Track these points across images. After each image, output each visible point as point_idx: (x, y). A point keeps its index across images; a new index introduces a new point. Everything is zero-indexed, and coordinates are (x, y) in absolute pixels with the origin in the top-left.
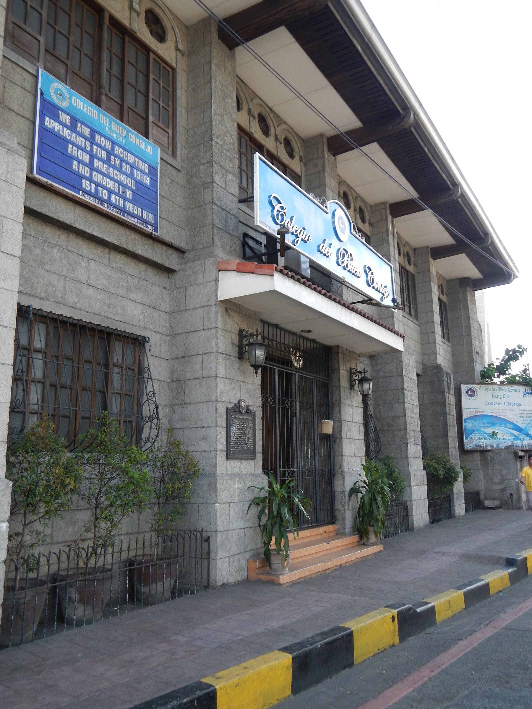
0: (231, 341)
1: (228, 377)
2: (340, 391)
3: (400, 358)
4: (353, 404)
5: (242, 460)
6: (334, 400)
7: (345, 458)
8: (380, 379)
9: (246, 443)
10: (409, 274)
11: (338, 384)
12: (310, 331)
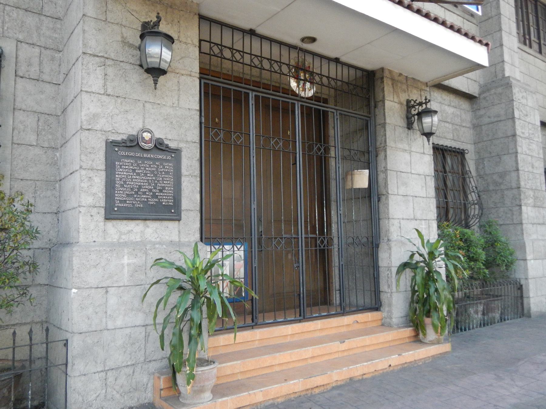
0: (119, 39)
1: (109, 91)
2: (385, 130)
3: (510, 95)
4: (412, 149)
5: (148, 222)
6: (378, 144)
7: (396, 222)
8: (483, 127)
9: (154, 196)
10: (538, 3)
11: (383, 122)
12: (313, 40)
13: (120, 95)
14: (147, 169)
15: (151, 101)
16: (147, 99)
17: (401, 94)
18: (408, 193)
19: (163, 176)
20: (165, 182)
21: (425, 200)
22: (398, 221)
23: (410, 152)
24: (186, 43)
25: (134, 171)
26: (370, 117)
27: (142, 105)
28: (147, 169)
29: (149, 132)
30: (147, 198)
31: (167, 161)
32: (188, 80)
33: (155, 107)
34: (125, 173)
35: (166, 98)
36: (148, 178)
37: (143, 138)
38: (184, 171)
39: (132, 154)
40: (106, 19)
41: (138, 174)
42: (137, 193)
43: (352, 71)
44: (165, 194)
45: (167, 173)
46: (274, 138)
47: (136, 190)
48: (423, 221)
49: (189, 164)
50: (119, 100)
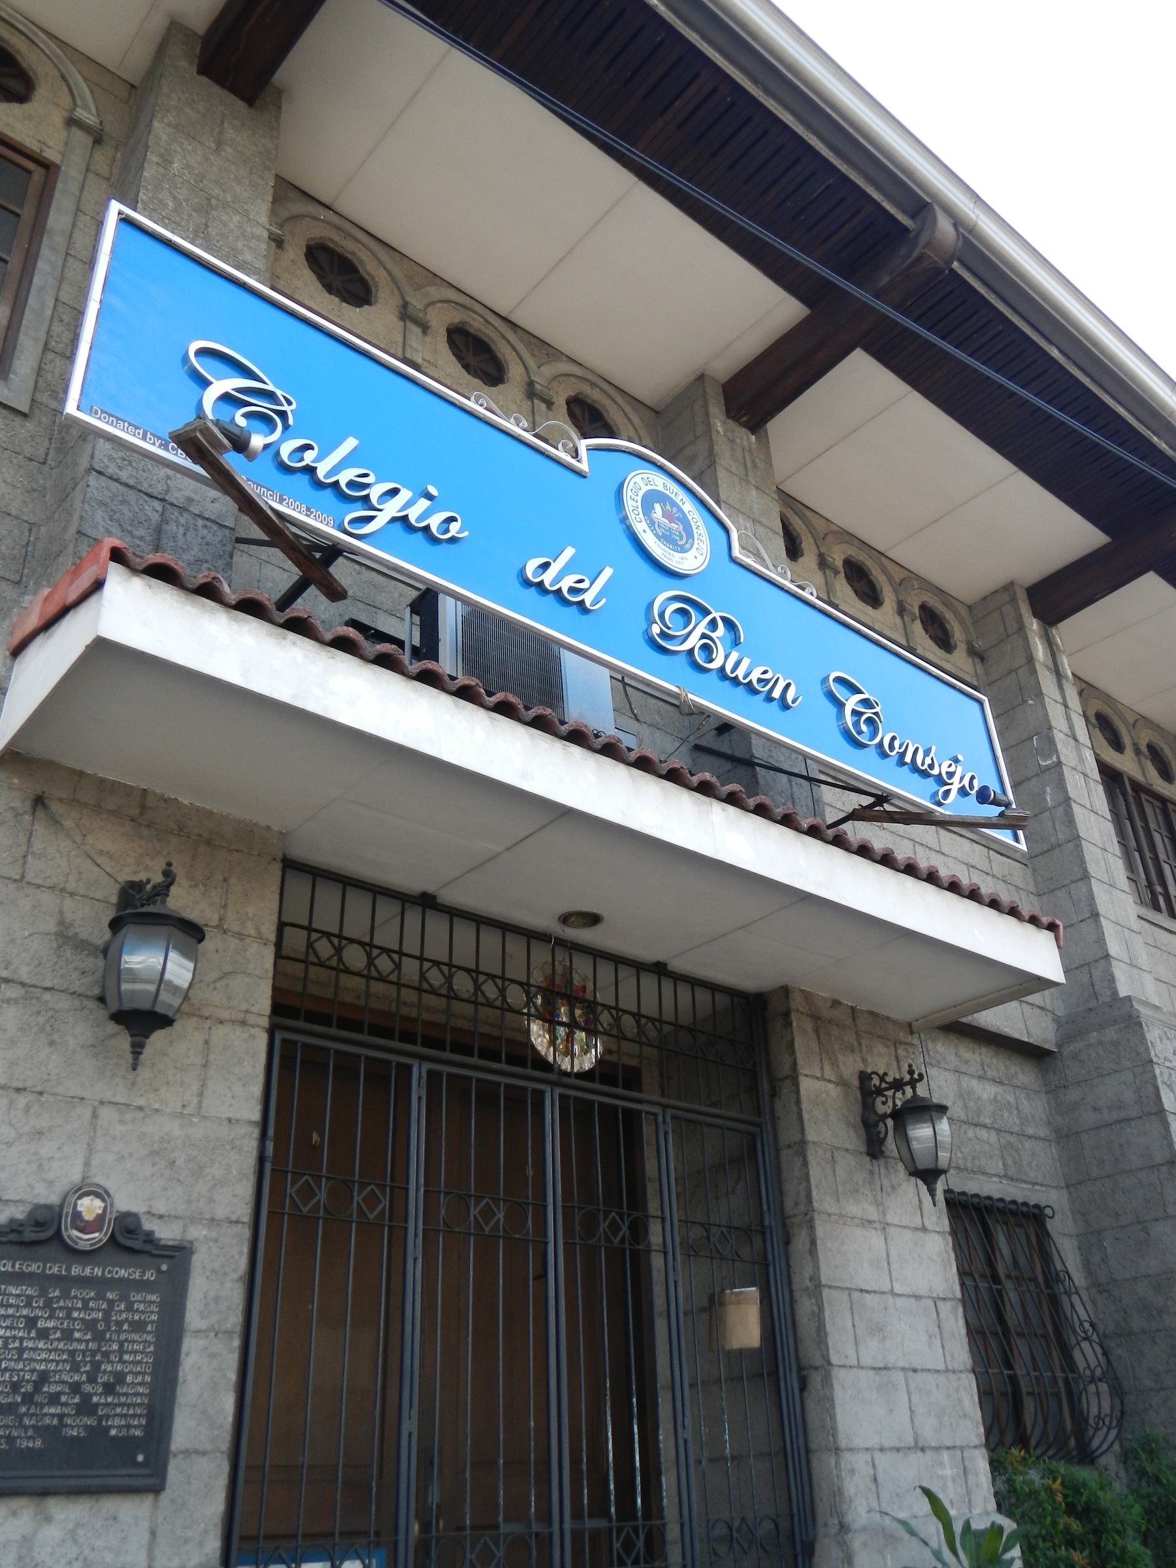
0: (51, 926)
2: (805, 1164)
3: (1141, 1049)
4: (890, 1218)
6: (789, 1203)
7: (859, 1462)
8: (1084, 1138)
9: (86, 1407)
10: (1170, 806)
11: (797, 1138)
12: (593, 919)
13: (28, 1084)
14: (75, 1314)
15: (118, 1099)
16: (108, 1095)
17: (841, 1057)
18: (892, 1360)
19: (123, 1337)
20: (126, 1357)
21: (941, 1379)
22: (868, 1457)
23: (885, 1226)
24: (240, 936)
25: (31, 1322)
26: (759, 1125)
27: (88, 1113)
29: (98, 1195)
30: (61, 1417)
31: (142, 1286)
32: (236, 1036)
33: (128, 1117)
35: (163, 1090)
36: (75, 1345)
37: (77, 1215)
38: (193, 1317)
39: (34, 1268)
40: (23, 877)
41: (44, 1334)
42: (28, 1399)
43: (703, 997)
44: (123, 1399)
45: (138, 1327)
46: (479, 1199)
47: (29, 1388)
48: (945, 1455)
49: (212, 1294)
50: (22, 1101)
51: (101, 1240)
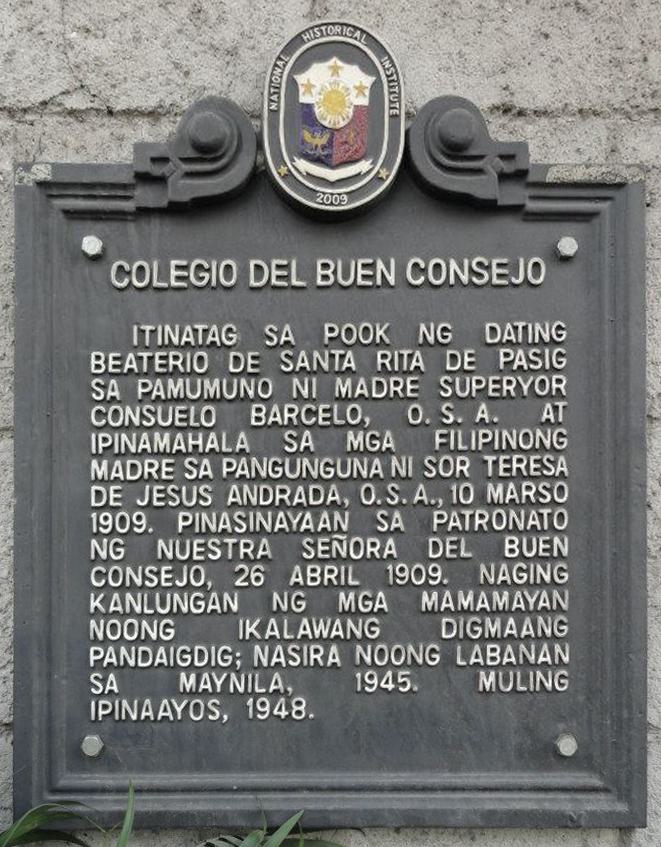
14: (343, 387)
19: (478, 440)
28: (343, 387)
30: (347, 643)
31: (510, 297)
34: (162, 442)
41: (269, 439)
51: (378, 179)
